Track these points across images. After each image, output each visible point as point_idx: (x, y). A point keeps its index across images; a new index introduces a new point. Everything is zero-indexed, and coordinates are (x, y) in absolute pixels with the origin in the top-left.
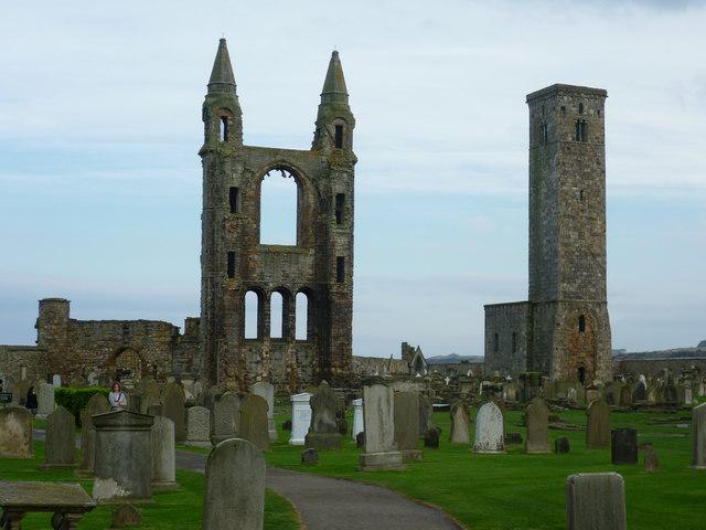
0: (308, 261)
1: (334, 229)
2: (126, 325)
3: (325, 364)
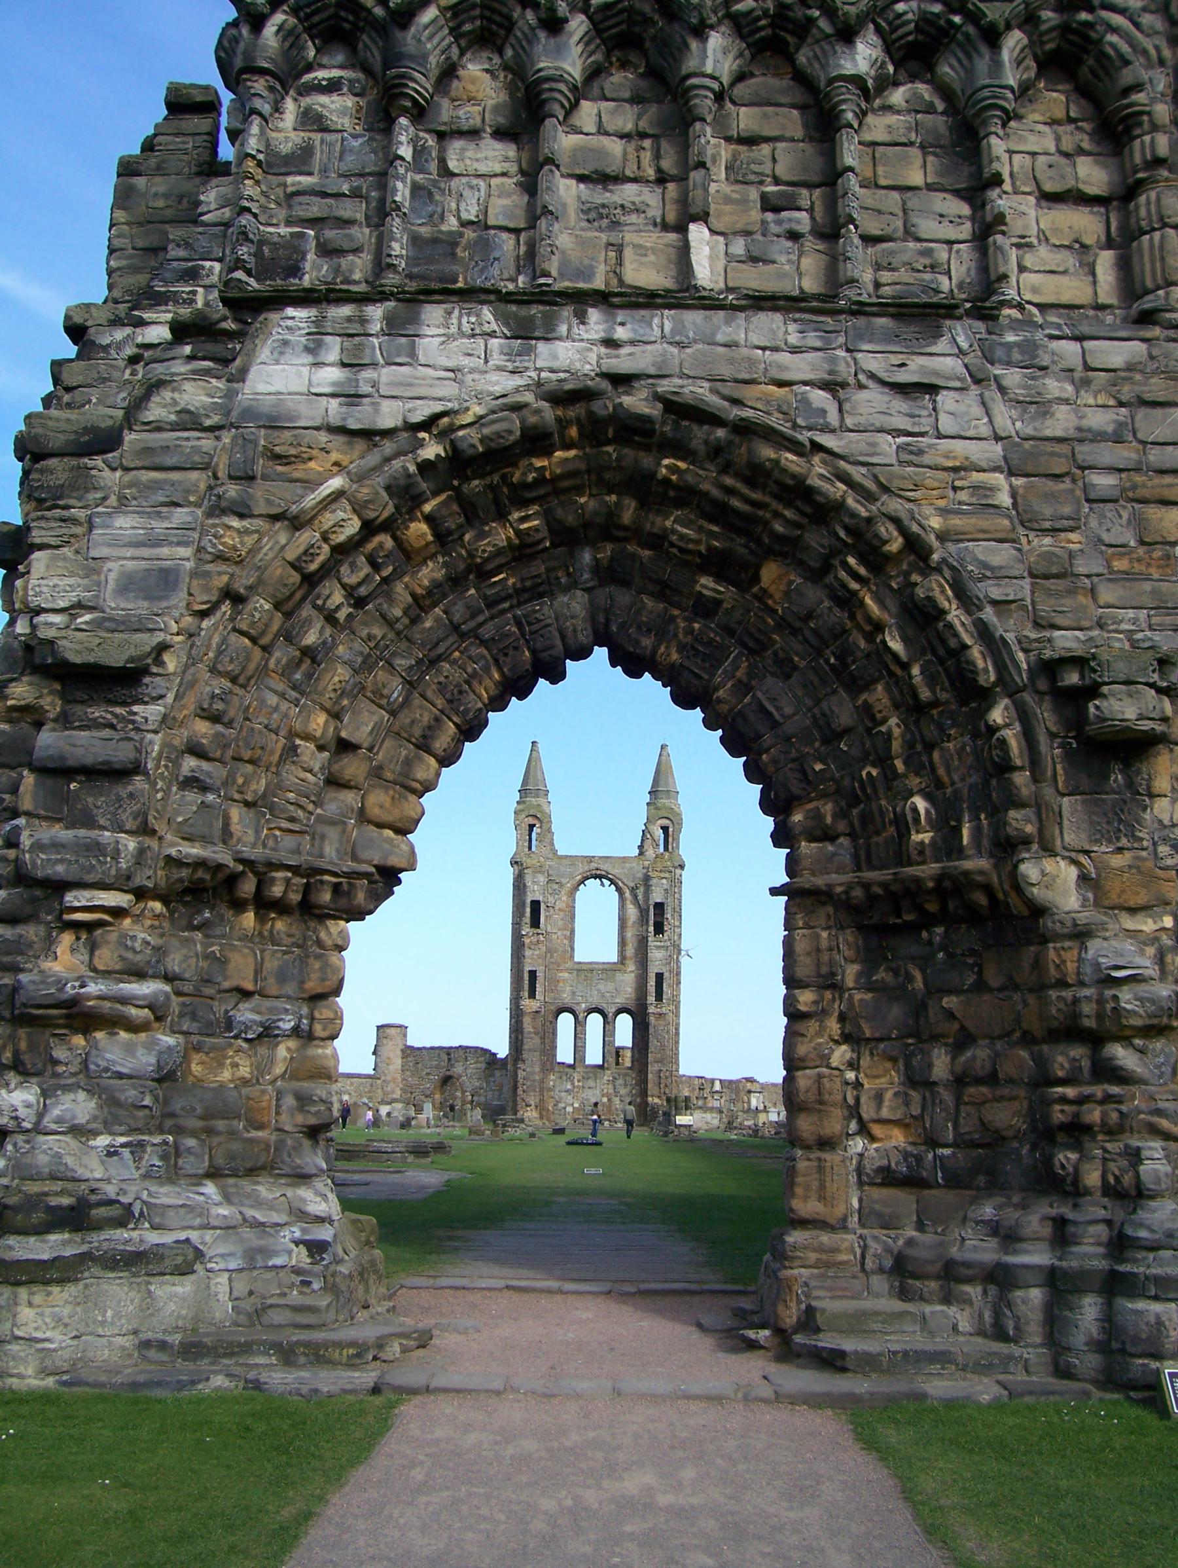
0: (628, 980)
1: (652, 941)
2: (448, 1051)
3: (644, 1093)
